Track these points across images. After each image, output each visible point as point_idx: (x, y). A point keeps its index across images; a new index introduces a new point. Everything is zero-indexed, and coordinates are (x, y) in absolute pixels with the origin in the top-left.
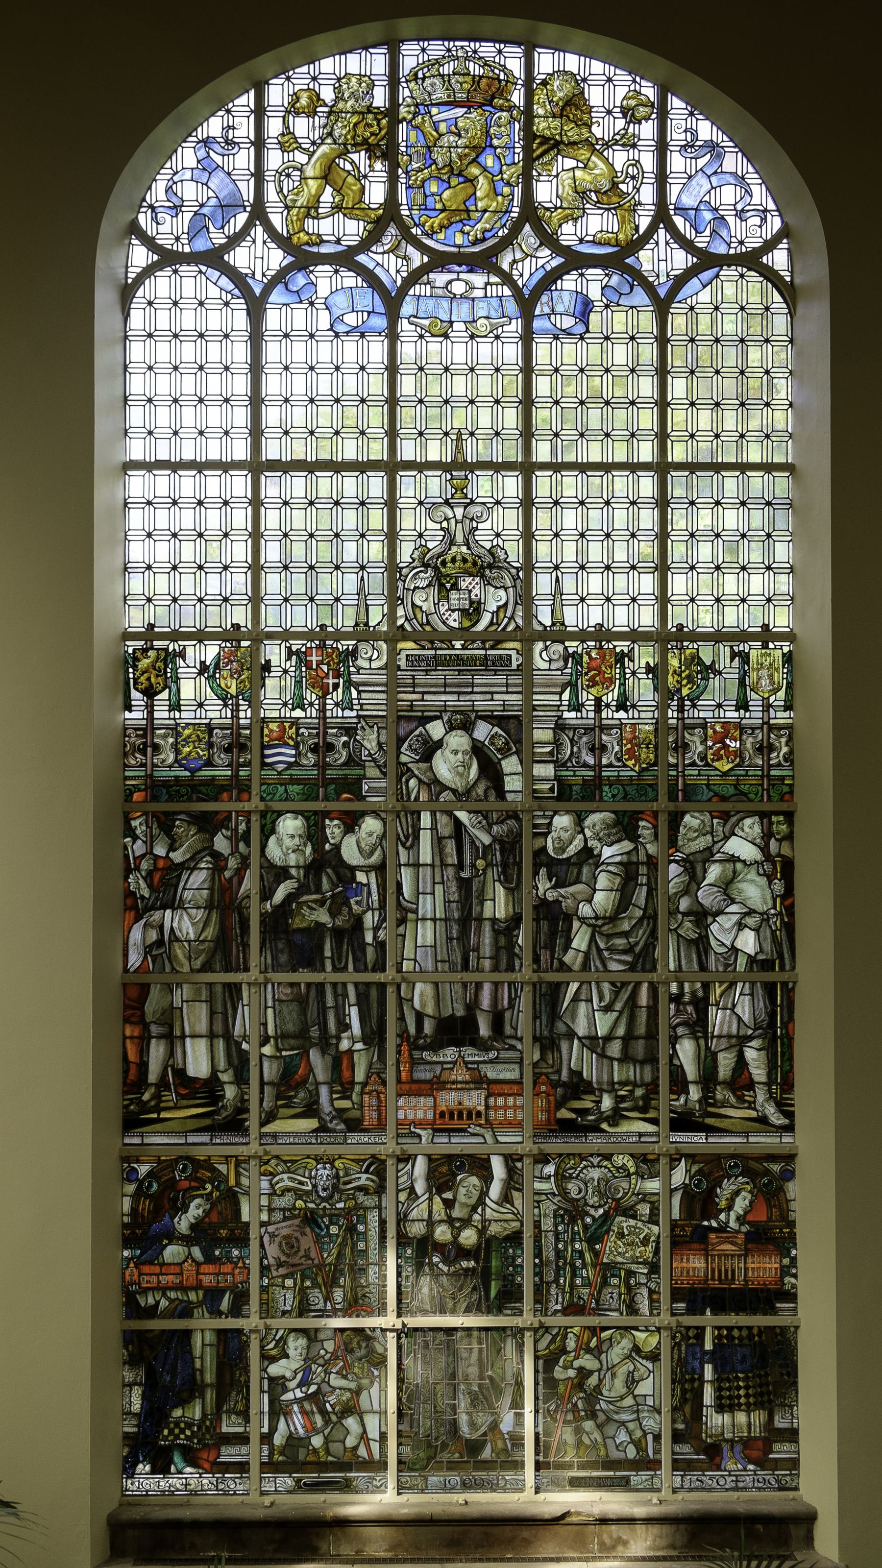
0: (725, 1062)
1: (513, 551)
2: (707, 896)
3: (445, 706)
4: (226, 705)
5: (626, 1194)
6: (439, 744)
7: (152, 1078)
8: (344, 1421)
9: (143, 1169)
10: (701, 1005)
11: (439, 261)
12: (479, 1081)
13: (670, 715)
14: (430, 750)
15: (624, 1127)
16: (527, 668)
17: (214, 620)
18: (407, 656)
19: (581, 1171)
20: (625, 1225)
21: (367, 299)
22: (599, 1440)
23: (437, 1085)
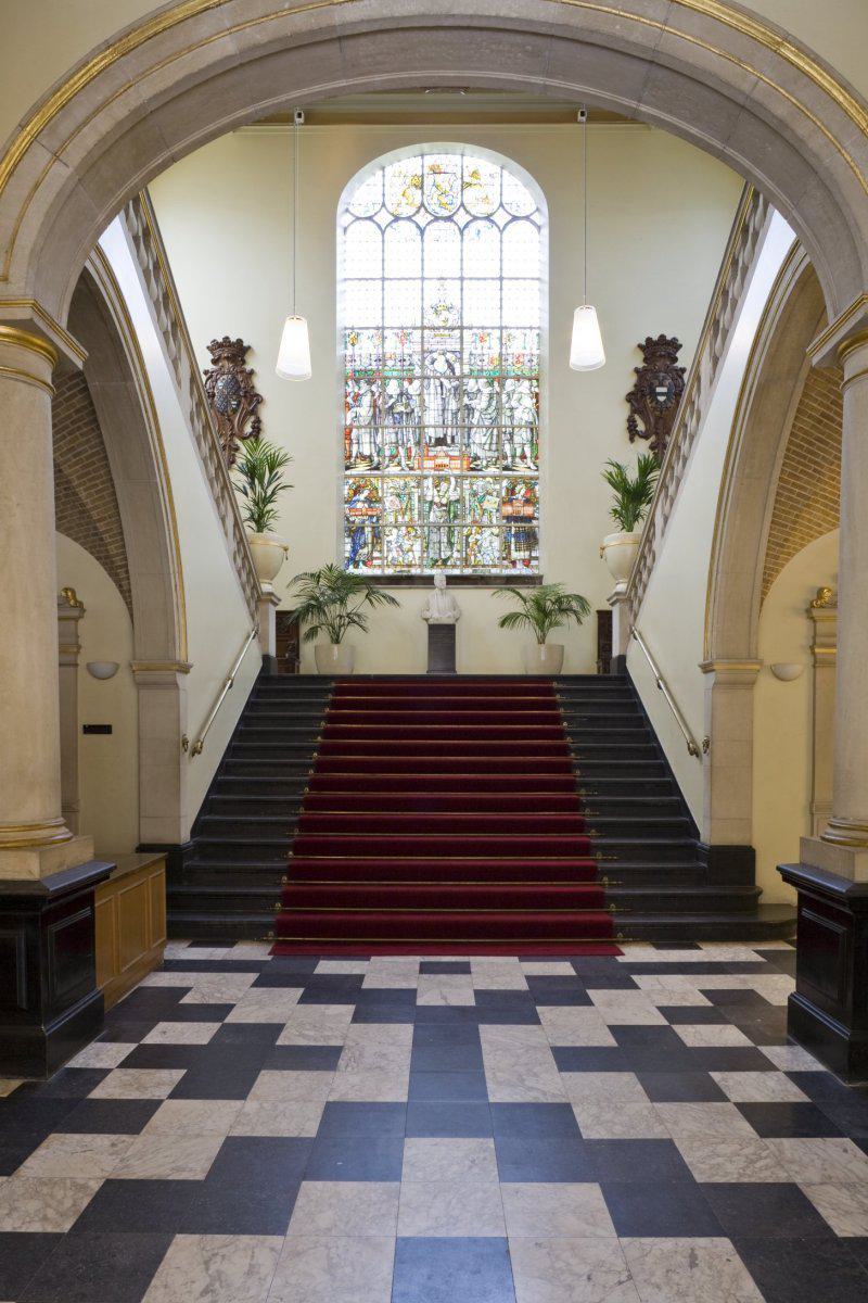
0: (519, 453)
7: (354, 455)
10: (512, 435)
11: (437, 219)
12: (447, 456)
15: (489, 469)
23: (435, 457)
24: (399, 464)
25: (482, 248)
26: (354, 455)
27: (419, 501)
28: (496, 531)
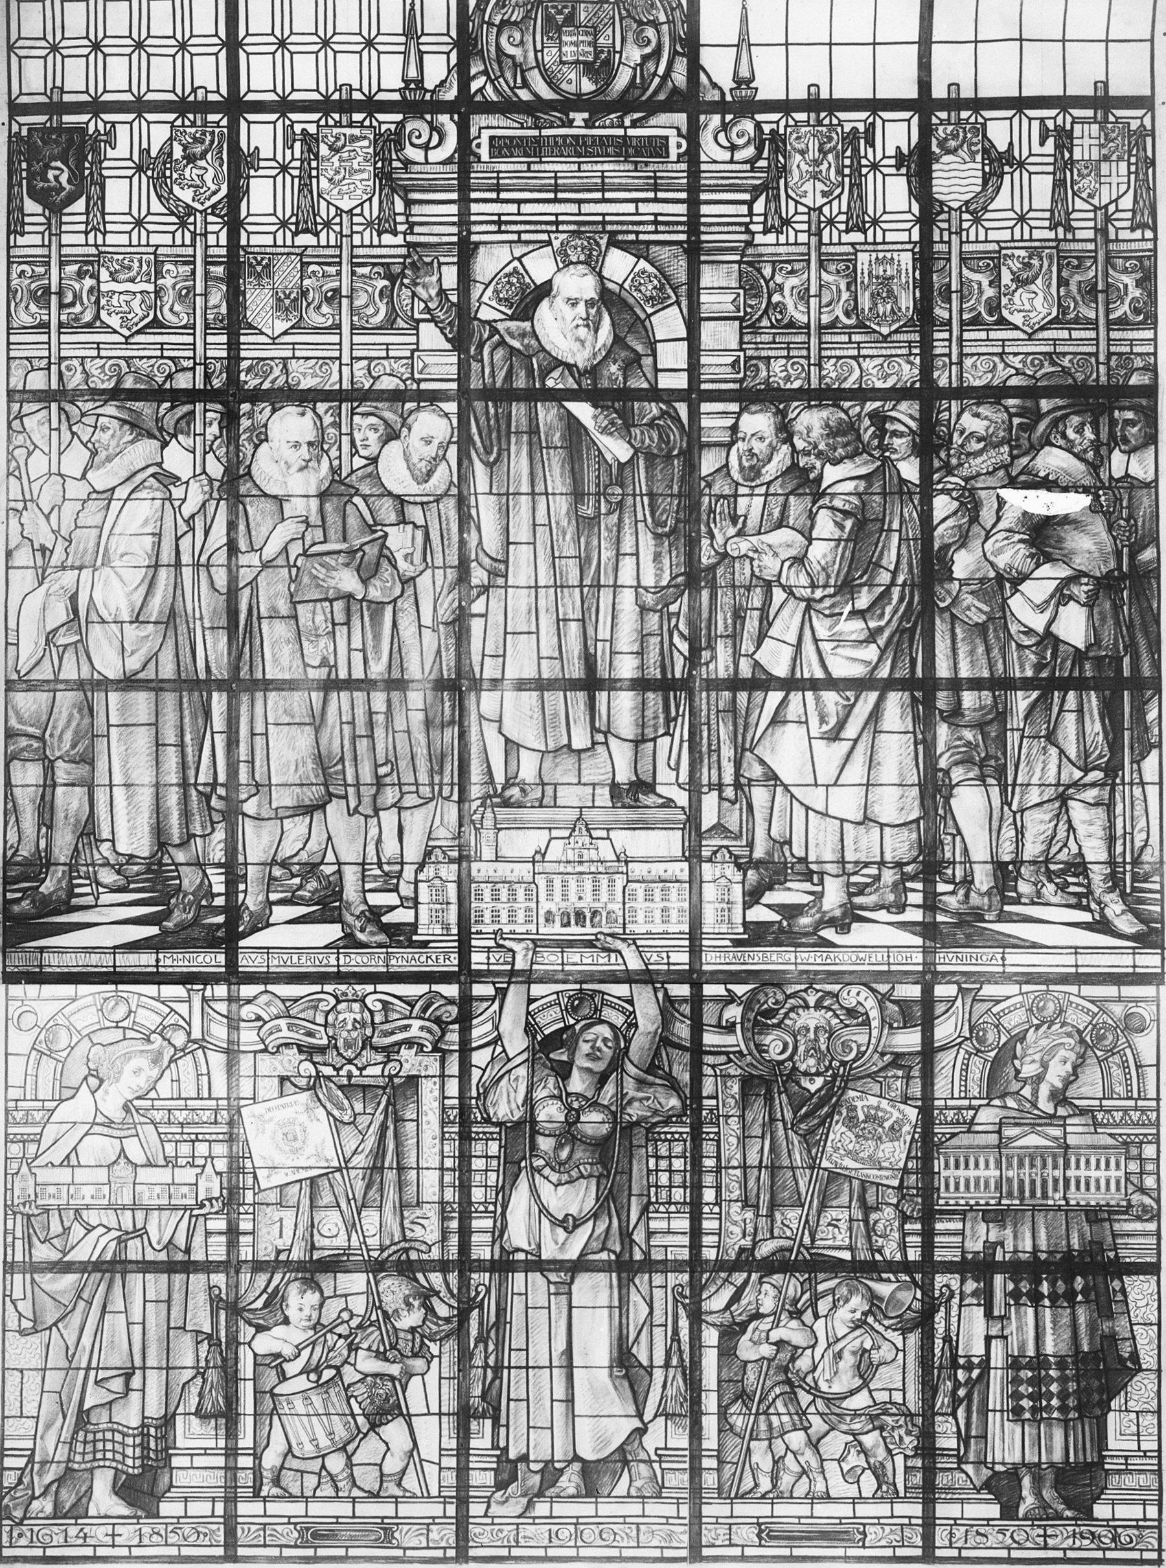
3: (557, 223)
4: (183, 224)
5: (860, 1054)
6: (545, 290)
8: (381, 1430)
13: (936, 238)
18: (492, 138)
19: (786, 1015)
20: (859, 1104)
22: (814, 1464)
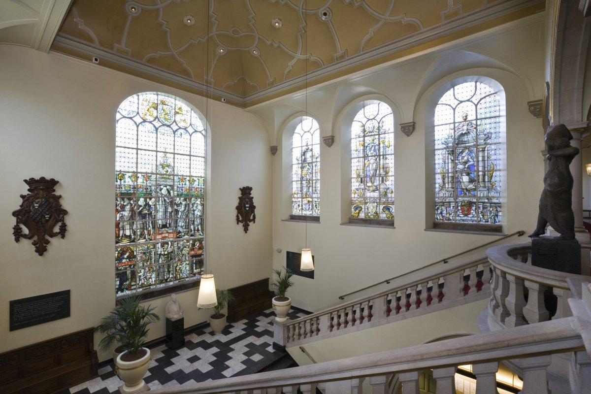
0: (196, 228)
1: (172, 165)
2: (194, 208)
7: (121, 236)
9: (119, 249)
10: (194, 221)
11: (164, 125)
12: (167, 232)
14: (161, 189)
15: (185, 237)
16: (174, 179)
17: (131, 170)
21: (153, 128)
23: (162, 233)
24: (145, 238)
25: (182, 143)
26: (121, 236)
27: (155, 254)
28: (187, 262)
